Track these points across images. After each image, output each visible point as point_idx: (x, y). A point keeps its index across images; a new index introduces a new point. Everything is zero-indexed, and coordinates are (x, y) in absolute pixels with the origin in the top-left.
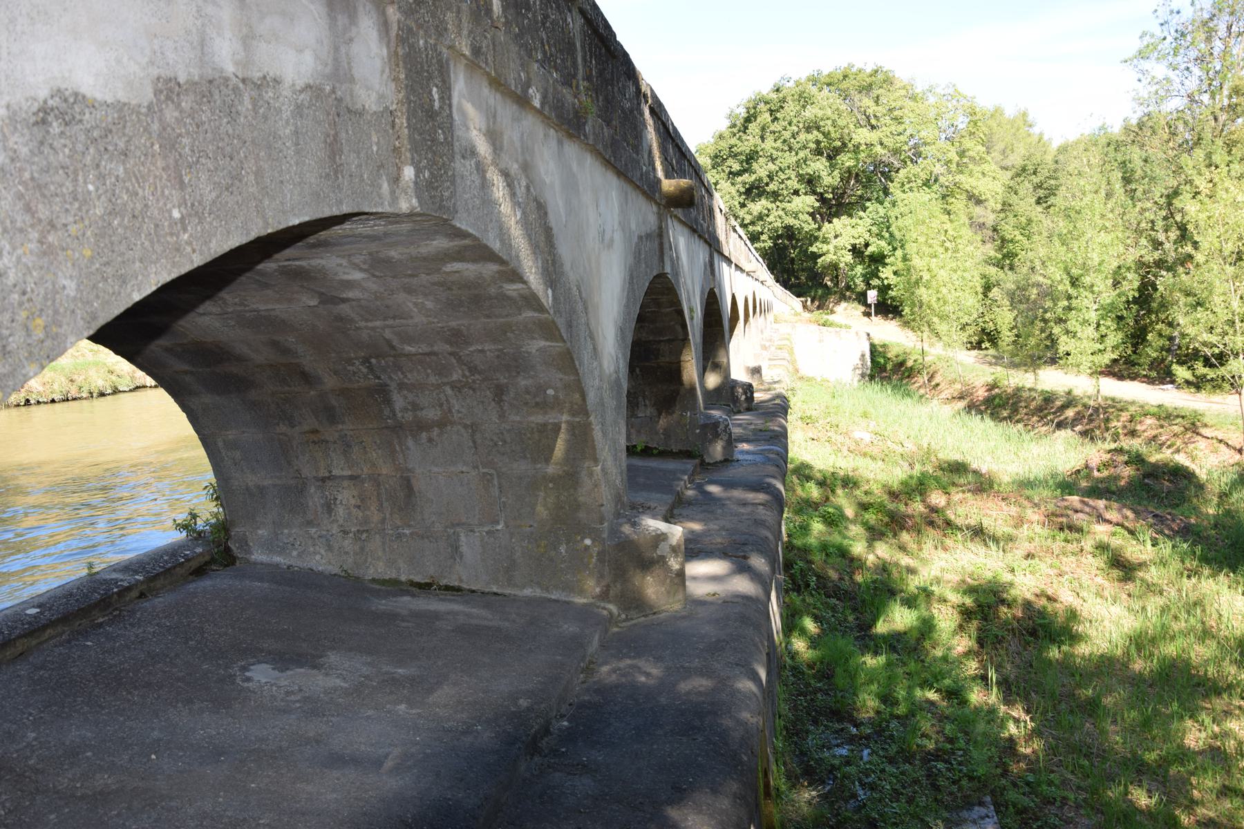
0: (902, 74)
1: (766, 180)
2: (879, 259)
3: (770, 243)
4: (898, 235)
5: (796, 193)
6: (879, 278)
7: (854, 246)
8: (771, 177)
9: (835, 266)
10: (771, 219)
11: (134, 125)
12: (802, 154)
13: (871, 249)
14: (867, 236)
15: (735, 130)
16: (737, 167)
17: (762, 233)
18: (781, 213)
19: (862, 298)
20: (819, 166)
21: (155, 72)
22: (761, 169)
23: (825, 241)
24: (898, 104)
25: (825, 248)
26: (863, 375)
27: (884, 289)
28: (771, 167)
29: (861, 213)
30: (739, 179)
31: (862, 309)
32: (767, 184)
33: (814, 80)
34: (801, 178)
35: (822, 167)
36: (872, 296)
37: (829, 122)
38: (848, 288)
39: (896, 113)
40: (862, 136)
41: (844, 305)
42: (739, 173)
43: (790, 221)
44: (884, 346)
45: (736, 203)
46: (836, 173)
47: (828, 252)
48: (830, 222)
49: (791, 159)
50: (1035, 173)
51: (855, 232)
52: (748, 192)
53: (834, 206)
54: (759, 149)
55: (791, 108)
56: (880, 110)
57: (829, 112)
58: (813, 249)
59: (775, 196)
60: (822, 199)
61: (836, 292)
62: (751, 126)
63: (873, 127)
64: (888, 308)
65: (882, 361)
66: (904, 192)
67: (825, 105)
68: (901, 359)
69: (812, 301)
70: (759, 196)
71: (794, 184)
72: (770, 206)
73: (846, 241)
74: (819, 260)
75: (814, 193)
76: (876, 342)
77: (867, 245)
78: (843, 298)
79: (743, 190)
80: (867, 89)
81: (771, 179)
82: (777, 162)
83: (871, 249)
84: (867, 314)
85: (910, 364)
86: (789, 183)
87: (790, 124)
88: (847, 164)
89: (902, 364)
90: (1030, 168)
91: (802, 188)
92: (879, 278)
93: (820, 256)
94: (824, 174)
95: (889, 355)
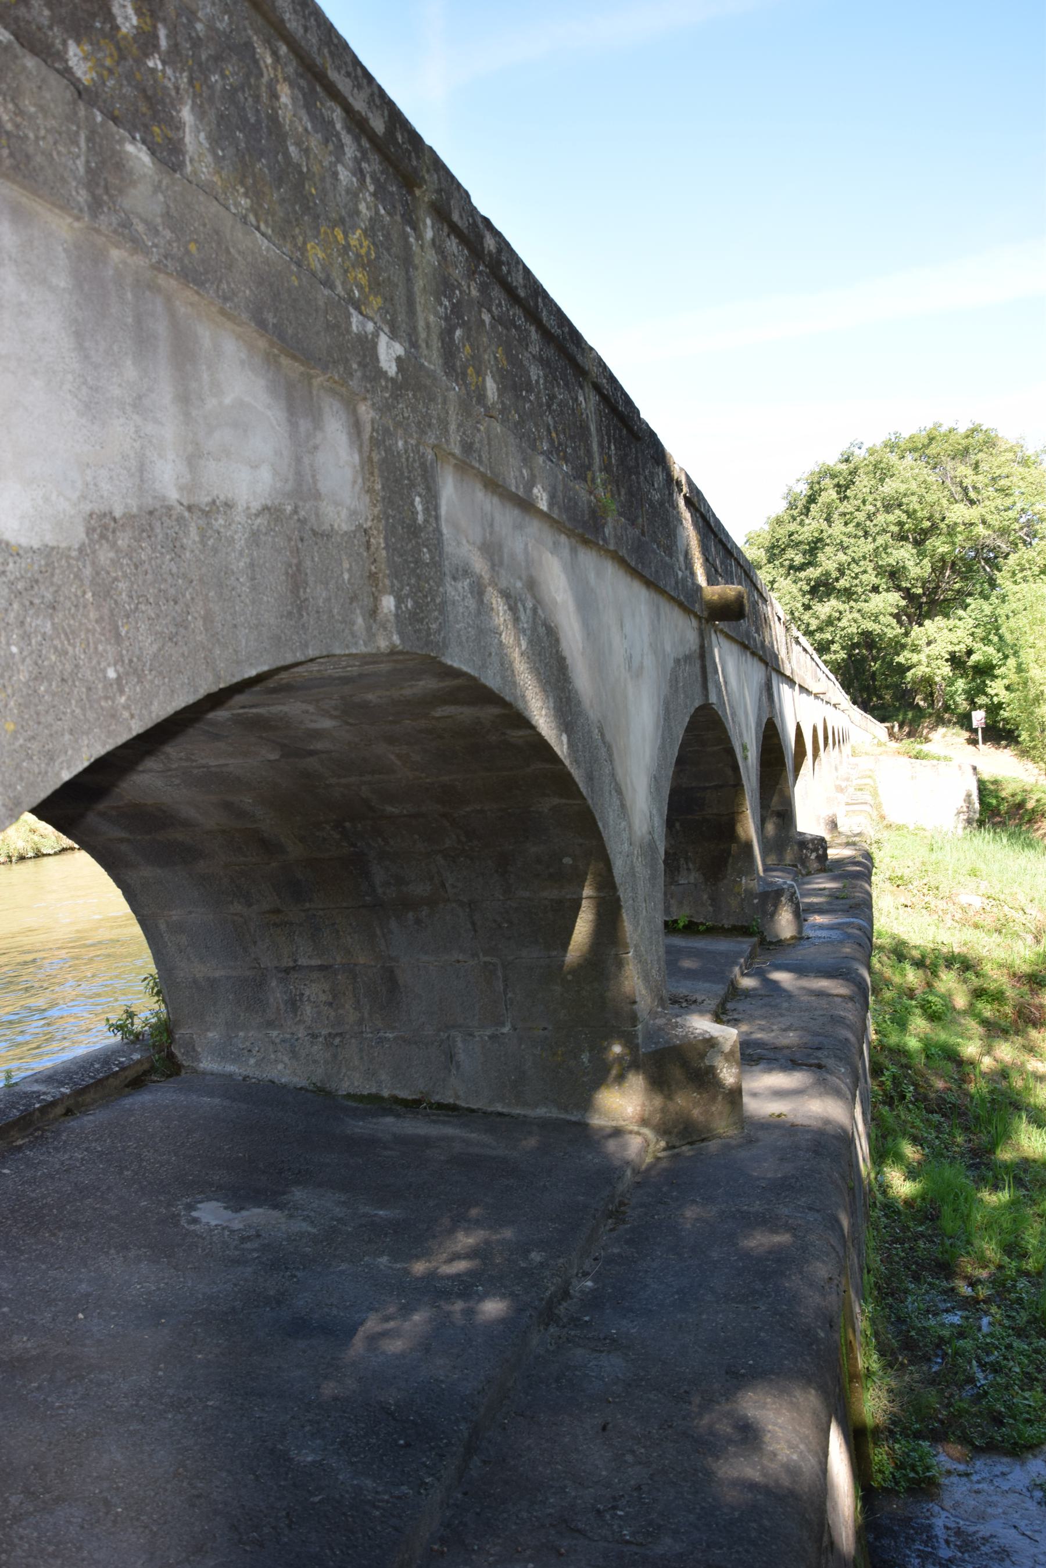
0: (1007, 433)
1: (835, 574)
2: (985, 671)
3: (843, 655)
4: (1008, 637)
5: (875, 589)
6: (986, 694)
7: (950, 653)
9: (928, 681)
10: (844, 623)
11: (63, 572)
12: (880, 540)
13: (974, 658)
14: (969, 641)
15: (795, 513)
16: (799, 559)
17: (833, 642)
18: (857, 615)
19: (965, 721)
20: (903, 554)
21: (87, 507)
22: (828, 561)
23: (916, 649)
24: (1005, 471)
25: (915, 658)
26: (969, 821)
27: (994, 709)
28: (842, 557)
29: (960, 612)
30: (802, 575)
31: (966, 735)
32: (837, 580)
33: (891, 446)
34: (880, 570)
35: (907, 556)
36: (979, 718)
37: (915, 498)
38: (947, 708)
39: (1003, 482)
40: (959, 513)
41: (941, 730)
42: (802, 568)
43: (869, 625)
44: (995, 782)
45: (799, 605)
46: (926, 561)
47: (919, 663)
48: (921, 625)
49: (867, 547)
51: (953, 637)
52: (813, 591)
53: (924, 604)
54: (825, 535)
56: (981, 480)
57: (914, 486)
58: (900, 659)
59: (848, 594)
60: (908, 595)
61: (931, 715)
63: (972, 502)
64: (999, 733)
65: (994, 802)
66: (1015, 582)
67: (909, 477)
68: (1019, 798)
69: (901, 727)
70: (829, 595)
72: (842, 607)
73: (942, 648)
74: (909, 674)
75: (899, 588)
76: (986, 776)
77: (970, 652)
78: (940, 721)
79: (807, 588)
80: (963, 453)
81: (843, 574)
84: (973, 742)
85: (1030, 805)
86: (864, 578)
87: (864, 502)
88: (940, 550)
89: (1021, 805)
91: (883, 583)
92: (986, 694)
93: (909, 668)
94: (910, 564)
95: (1003, 794)
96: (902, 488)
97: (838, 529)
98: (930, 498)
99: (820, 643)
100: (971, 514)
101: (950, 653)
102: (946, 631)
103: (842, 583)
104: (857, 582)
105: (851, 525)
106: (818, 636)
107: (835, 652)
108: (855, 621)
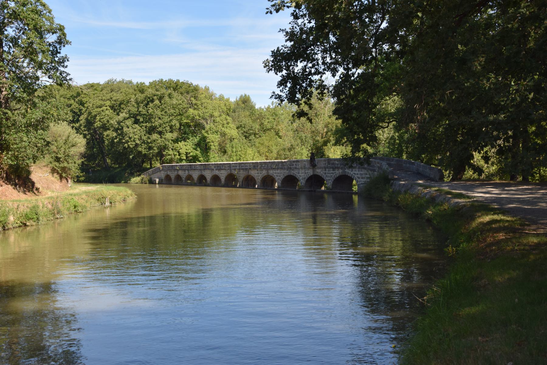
3: (156, 151)
7: (187, 153)
12: (171, 118)
14: (192, 149)
28: (160, 121)
30: (144, 124)
42: (142, 122)
43: (167, 143)
50: (244, 128)
55: (167, 98)
57: (181, 102)
59: (160, 133)
62: (151, 105)
67: (177, 99)
71: (168, 128)
77: (189, 153)
81: (160, 126)
83: (191, 154)
90: (243, 126)
98: (186, 106)
100: (196, 112)
103: (160, 129)
106: (150, 145)
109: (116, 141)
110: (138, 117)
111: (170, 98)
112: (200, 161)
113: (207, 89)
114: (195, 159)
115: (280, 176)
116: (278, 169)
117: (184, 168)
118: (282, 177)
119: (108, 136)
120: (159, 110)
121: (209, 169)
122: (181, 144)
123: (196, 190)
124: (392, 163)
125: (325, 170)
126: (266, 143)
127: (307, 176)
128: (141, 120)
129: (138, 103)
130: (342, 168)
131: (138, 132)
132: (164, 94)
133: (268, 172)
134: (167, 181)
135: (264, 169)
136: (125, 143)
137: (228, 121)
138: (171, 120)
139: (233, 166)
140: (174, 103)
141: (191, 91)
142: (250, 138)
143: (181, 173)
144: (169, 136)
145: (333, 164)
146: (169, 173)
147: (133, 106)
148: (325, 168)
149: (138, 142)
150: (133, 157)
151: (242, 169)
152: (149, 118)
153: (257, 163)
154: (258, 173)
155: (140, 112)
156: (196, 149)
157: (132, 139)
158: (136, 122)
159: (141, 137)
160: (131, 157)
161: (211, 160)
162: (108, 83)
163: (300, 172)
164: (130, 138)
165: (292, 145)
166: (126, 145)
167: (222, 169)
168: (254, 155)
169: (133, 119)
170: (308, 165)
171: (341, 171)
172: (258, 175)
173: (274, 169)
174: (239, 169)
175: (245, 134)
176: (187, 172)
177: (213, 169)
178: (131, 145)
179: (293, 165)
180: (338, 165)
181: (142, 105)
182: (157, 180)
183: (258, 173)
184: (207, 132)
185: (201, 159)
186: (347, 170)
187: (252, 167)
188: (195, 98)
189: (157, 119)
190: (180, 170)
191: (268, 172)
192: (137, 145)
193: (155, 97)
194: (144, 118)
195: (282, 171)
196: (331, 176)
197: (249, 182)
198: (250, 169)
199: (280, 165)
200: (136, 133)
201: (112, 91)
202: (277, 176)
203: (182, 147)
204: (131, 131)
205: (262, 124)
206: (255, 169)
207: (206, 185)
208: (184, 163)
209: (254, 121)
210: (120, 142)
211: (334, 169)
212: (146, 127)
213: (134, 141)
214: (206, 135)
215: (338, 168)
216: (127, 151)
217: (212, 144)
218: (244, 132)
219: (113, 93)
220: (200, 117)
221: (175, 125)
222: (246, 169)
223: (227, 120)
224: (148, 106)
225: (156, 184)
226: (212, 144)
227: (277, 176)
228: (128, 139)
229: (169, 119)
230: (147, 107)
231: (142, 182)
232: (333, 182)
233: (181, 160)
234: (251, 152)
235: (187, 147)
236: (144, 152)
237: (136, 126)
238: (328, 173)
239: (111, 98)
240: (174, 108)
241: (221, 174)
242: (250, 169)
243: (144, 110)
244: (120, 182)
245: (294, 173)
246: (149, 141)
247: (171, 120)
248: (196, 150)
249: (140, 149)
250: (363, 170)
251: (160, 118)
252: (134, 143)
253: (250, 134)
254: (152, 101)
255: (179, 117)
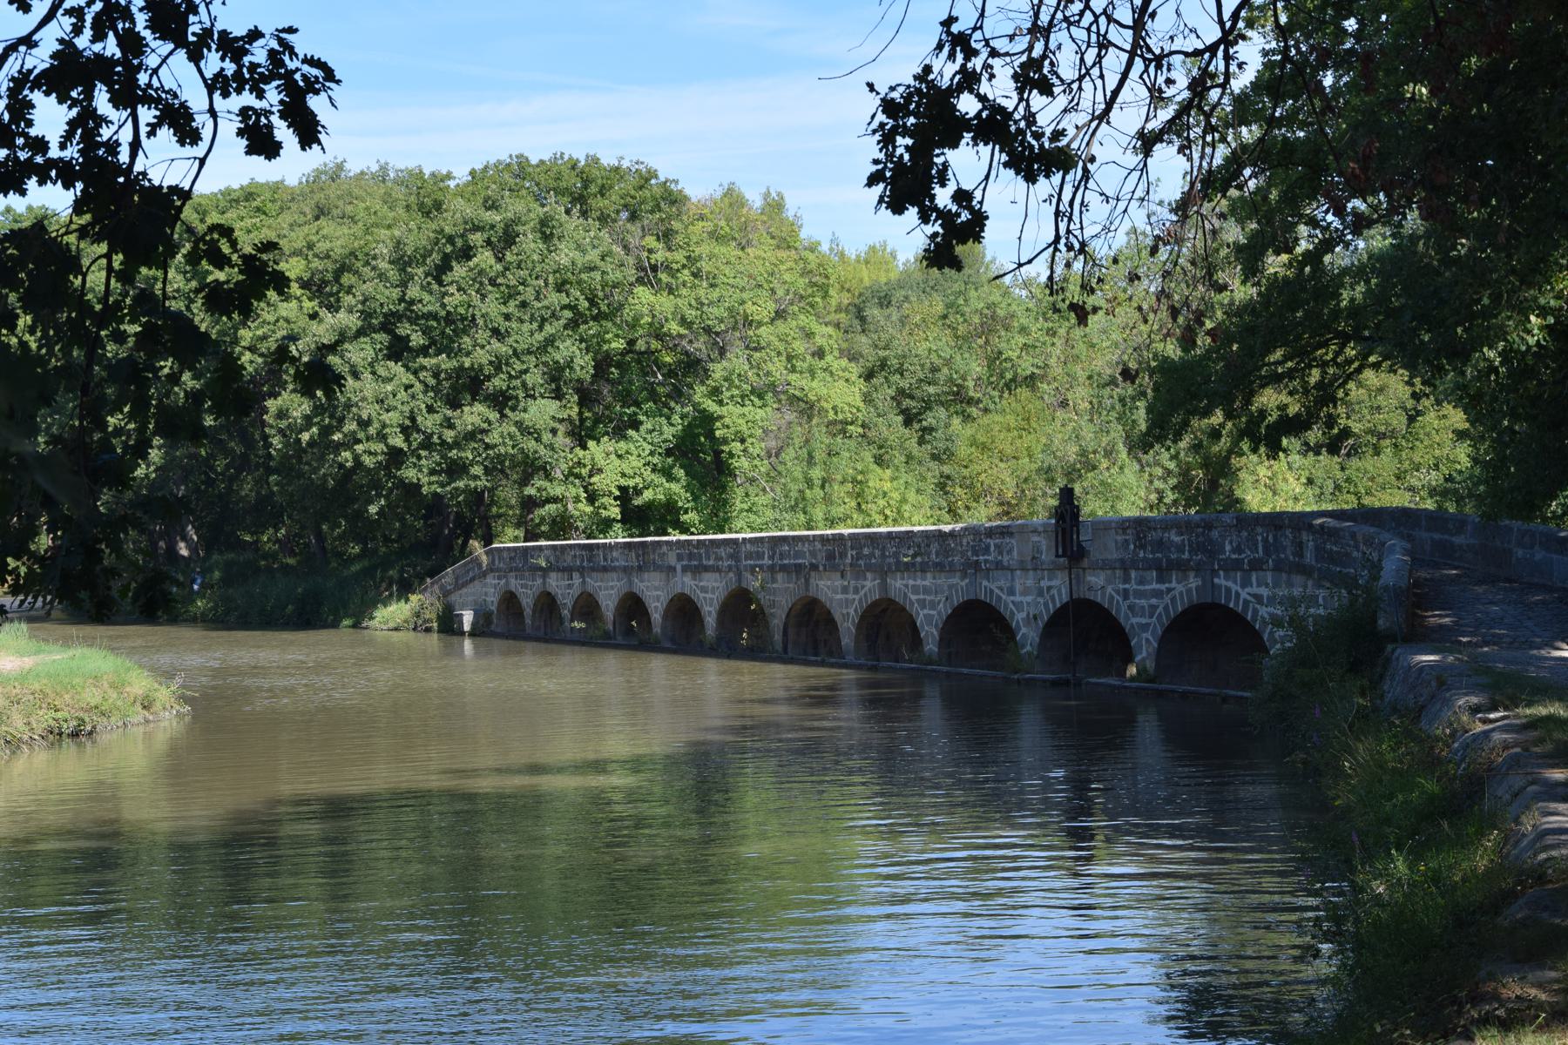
8: (498, 364)
10: (493, 438)
20: (567, 349)
22: (480, 352)
25: (557, 490)
28: (495, 344)
30: (426, 361)
32: (488, 378)
42: (424, 351)
43: (531, 445)
55: (529, 243)
57: (593, 256)
59: (501, 401)
62: (459, 271)
66: (721, 403)
67: (580, 245)
71: (535, 378)
72: (494, 416)
73: (607, 481)
77: (638, 492)
81: (498, 369)
82: (510, 340)
83: (648, 495)
94: (579, 361)
96: (581, 261)
97: (492, 307)
98: (614, 276)
99: (453, 462)
100: (665, 303)
101: (620, 488)
102: (613, 457)
103: (498, 382)
104: (517, 382)
105: (512, 303)
106: (453, 453)
107: (476, 478)
108: (511, 437)
109: (305, 437)
110: (404, 329)
111: (547, 238)
112: (685, 529)
113: (775, 206)
114: (666, 515)
115: (933, 605)
116: (924, 569)
117: (568, 559)
118: (944, 610)
119: (282, 414)
120: (493, 295)
121: (658, 568)
122: (597, 450)
123: (659, 666)
124: (1458, 540)
125: (1127, 580)
126: (1004, 443)
127: (1045, 612)
128: (417, 339)
129: (402, 262)
130: (1198, 569)
131: (402, 395)
132: (517, 221)
133: (884, 586)
134: (522, 623)
135: (869, 568)
136: (338, 447)
137: (819, 341)
138: (550, 341)
139: (749, 556)
140: (564, 261)
141: (646, 202)
142: (929, 420)
143: (555, 583)
144: (542, 411)
145: (1160, 545)
146: (514, 584)
147: (382, 276)
148: (1125, 567)
149: (398, 441)
150: (381, 512)
151: (784, 568)
152: (449, 330)
153: (841, 535)
154: (845, 590)
155: (412, 302)
156: (668, 474)
157: (372, 430)
158: (398, 350)
159: (413, 419)
160: (373, 509)
161: (739, 524)
162: (317, 178)
163: (1018, 587)
164: (364, 424)
165: (1083, 453)
166: (346, 454)
167: (707, 569)
168: (904, 500)
169: (382, 337)
170: (1046, 548)
171: (1194, 582)
172: (845, 598)
173: (908, 567)
174: (772, 568)
175: (907, 403)
176: (577, 580)
177: (672, 569)
178: (370, 453)
179: (987, 550)
180: (1180, 549)
181: (420, 271)
182: (468, 618)
183: (845, 590)
184: (715, 392)
185: (690, 517)
186: (1220, 581)
187: (820, 559)
188: (666, 236)
189: (482, 335)
190: (550, 568)
191: (884, 586)
192: (396, 457)
193: (477, 238)
194: (426, 331)
195: (943, 581)
196: (1153, 608)
197: (811, 632)
198: (814, 567)
199: (934, 547)
200: (391, 402)
201: (320, 212)
202: (922, 604)
203: (601, 462)
204: (368, 394)
205: (995, 358)
206: (834, 568)
207: (647, 645)
208: (618, 536)
209: (963, 341)
210: (323, 445)
211: (1163, 570)
212: (436, 375)
213: (382, 437)
214: (711, 406)
215: (1182, 567)
216: (350, 487)
217: (736, 447)
218: (901, 392)
219: (322, 222)
220: (683, 322)
221: (569, 364)
222: (798, 568)
223: (809, 335)
224: (447, 278)
225: (462, 633)
226: (736, 447)
227: (922, 604)
228: (353, 426)
229: (539, 337)
230: (440, 283)
231: (418, 625)
232: (1163, 641)
233: (606, 525)
234: (887, 486)
235: (625, 462)
236: (430, 485)
237: (397, 368)
238: (1140, 594)
239: (310, 246)
240: (560, 287)
241: (704, 590)
242: (814, 567)
243: (426, 297)
244: (335, 625)
245: (992, 588)
246: (449, 435)
247: (550, 341)
248: (670, 477)
249: (410, 474)
250: (1298, 579)
251: (496, 332)
252: (380, 447)
253: (928, 405)
254: (466, 253)
255: (592, 329)
